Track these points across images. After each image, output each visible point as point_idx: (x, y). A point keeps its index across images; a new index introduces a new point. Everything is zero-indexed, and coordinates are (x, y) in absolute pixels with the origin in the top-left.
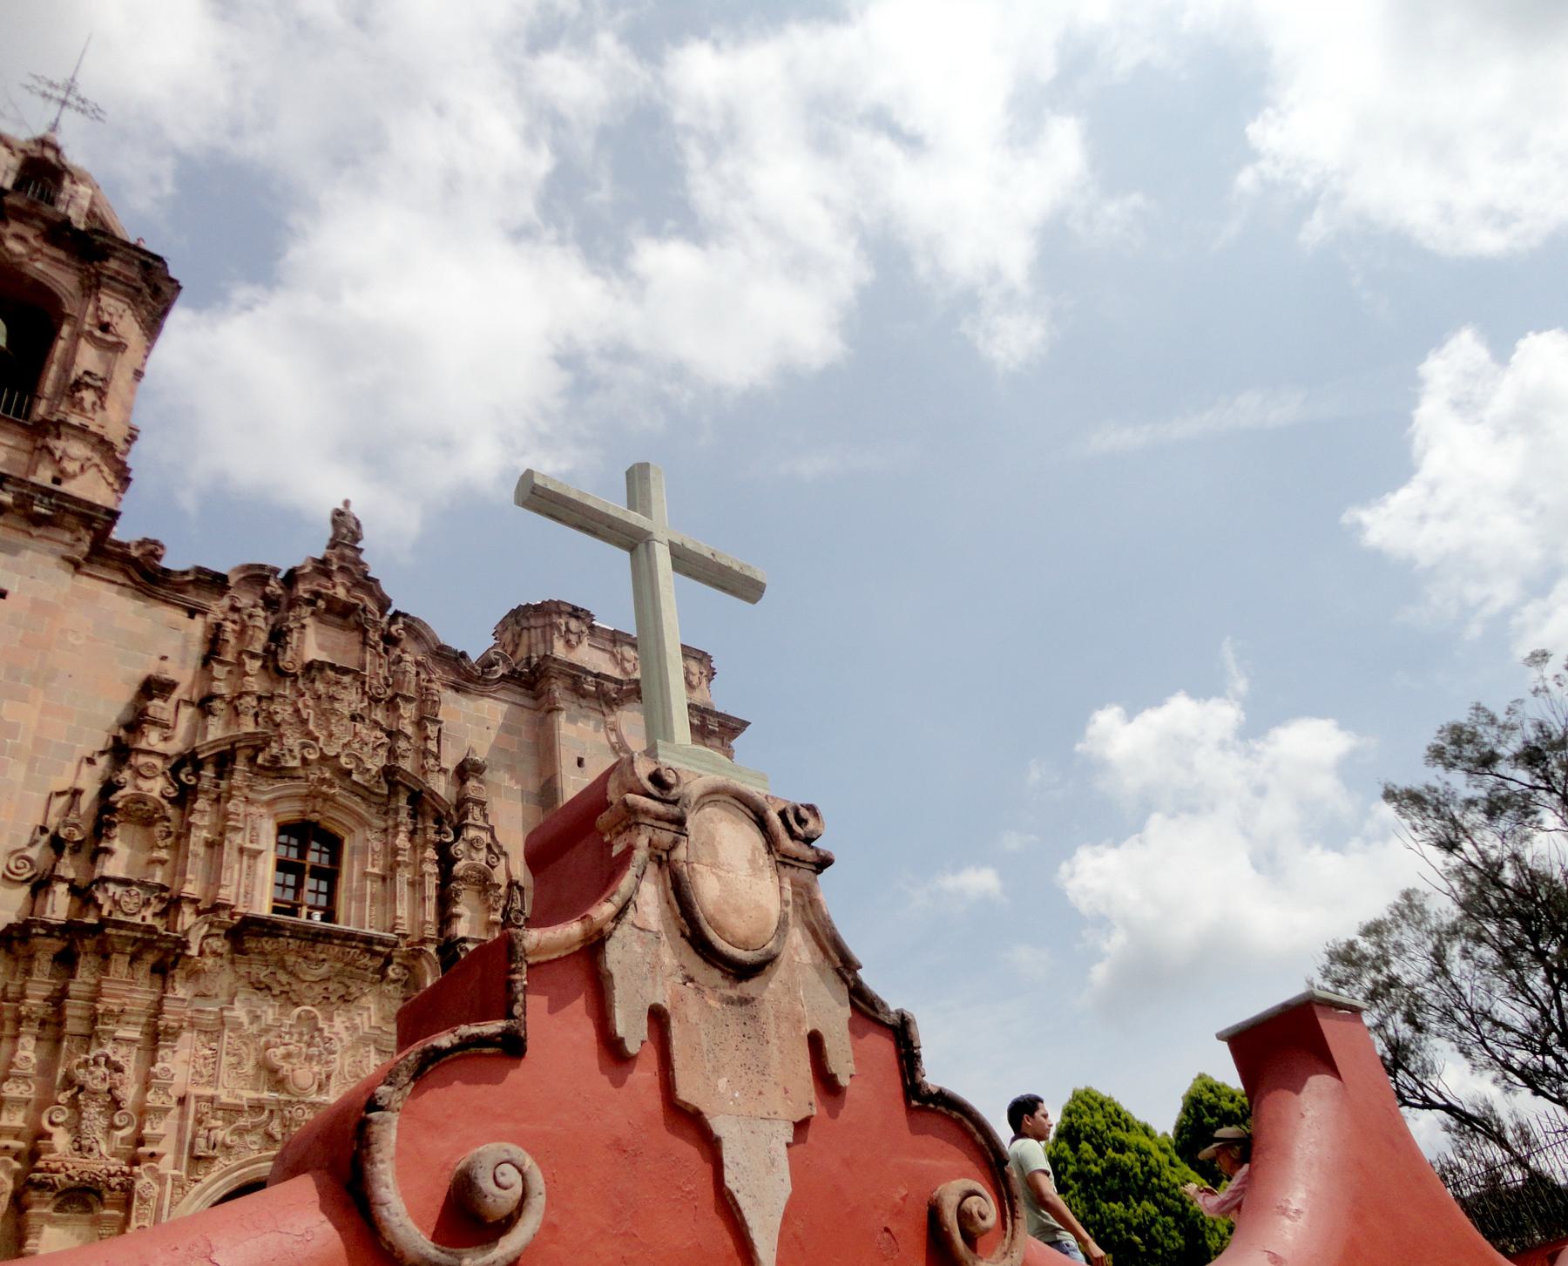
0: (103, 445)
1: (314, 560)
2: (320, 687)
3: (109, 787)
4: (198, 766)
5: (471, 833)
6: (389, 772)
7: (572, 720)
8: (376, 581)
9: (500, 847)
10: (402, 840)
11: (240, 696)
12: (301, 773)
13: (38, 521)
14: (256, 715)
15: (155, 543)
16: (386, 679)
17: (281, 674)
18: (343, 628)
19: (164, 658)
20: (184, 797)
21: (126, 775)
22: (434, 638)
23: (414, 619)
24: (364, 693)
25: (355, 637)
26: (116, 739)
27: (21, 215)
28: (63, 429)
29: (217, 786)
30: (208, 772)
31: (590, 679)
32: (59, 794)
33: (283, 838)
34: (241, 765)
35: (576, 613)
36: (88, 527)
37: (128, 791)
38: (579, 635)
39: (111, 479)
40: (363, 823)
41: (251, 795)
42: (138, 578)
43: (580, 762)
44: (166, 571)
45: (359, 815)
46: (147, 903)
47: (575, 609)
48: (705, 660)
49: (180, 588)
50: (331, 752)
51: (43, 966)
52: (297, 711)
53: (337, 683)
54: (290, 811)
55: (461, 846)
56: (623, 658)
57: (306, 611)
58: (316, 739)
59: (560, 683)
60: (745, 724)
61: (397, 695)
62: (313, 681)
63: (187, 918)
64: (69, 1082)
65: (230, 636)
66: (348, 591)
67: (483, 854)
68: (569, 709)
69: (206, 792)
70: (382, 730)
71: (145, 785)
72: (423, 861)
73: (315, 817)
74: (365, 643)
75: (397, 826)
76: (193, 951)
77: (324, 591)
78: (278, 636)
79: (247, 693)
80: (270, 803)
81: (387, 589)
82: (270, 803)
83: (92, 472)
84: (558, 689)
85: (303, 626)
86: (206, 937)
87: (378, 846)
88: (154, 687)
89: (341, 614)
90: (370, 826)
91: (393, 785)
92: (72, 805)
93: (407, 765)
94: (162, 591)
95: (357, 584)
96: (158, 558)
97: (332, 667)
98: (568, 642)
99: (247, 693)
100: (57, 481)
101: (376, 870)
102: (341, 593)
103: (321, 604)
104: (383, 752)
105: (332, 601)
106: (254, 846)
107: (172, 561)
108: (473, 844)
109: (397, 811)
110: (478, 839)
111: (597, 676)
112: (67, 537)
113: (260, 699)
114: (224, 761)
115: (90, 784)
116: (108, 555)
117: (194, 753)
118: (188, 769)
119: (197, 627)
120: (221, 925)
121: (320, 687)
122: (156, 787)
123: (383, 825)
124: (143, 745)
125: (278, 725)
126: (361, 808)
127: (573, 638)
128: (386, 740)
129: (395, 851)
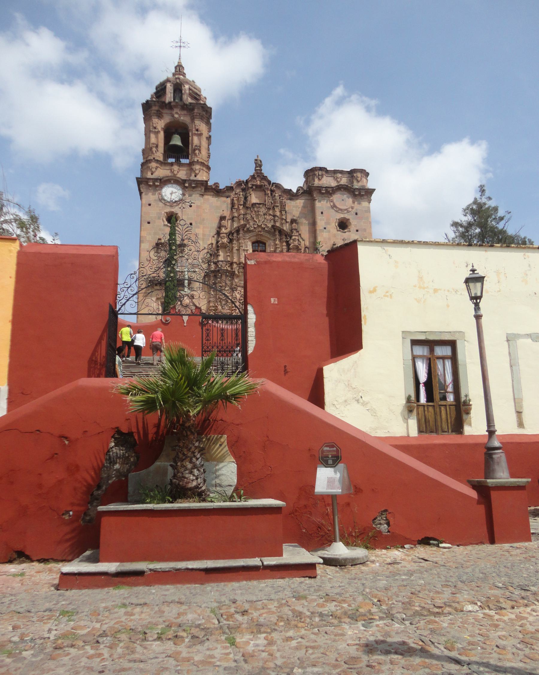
0: (202, 164)
1: (251, 176)
2: (256, 209)
3: (217, 242)
4: (233, 234)
5: (293, 237)
6: (273, 226)
7: (320, 201)
8: (266, 177)
9: (302, 238)
10: (277, 242)
11: (240, 215)
12: (254, 230)
13: (194, 188)
14: (244, 219)
15: (217, 183)
16: (271, 202)
17: (247, 208)
18: (261, 191)
19: (223, 211)
20: (231, 241)
21: (220, 239)
22: (283, 187)
23: (278, 184)
24: (266, 208)
25: (263, 193)
26: (217, 231)
27: (176, 106)
28: (194, 163)
29: (237, 237)
30: (235, 235)
31: (324, 189)
32: (209, 245)
33: (254, 245)
34: (241, 232)
35: (321, 169)
36: (203, 186)
37: (220, 242)
38: (322, 175)
39: (206, 170)
40: (269, 239)
41: (245, 238)
42: (216, 193)
43: (322, 213)
44: (220, 189)
45: (267, 237)
46: (226, 265)
47: (320, 168)
48: (363, 172)
49: (224, 192)
50: (259, 224)
51: (212, 278)
52: (252, 216)
53: (259, 207)
54: (254, 239)
55: (291, 241)
56: (337, 178)
57: (251, 190)
58: (256, 222)
59: (316, 192)
60: (374, 190)
61: (274, 206)
62: (254, 208)
63: (235, 266)
64: (219, 298)
65: (236, 202)
66: (260, 181)
67: (297, 242)
68: (319, 199)
69: (235, 239)
70: (272, 215)
71: (223, 240)
72: (283, 246)
73: (259, 239)
74: (265, 194)
75: (276, 239)
76: (237, 272)
77: (255, 183)
78: (246, 198)
79: (241, 214)
80: (249, 238)
81: (269, 178)
82: (249, 238)
83: (201, 171)
84: (315, 195)
85: (251, 194)
86: (238, 270)
87: (273, 244)
88: (222, 218)
89: (259, 188)
90: (271, 240)
91: (274, 229)
92: (212, 246)
93: (278, 224)
94: (221, 194)
95: (262, 179)
96: (219, 187)
97: (257, 203)
98: (319, 178)
99: (241, 214)
100: (195, 176)
101: (273, 250)
102: (258, 183)
103: (254, 187)
104: (272, 221)
105: (257, 186)
106: (247, 249)
107: (221, 187)
108: (294, 240)
109: (276, 235)
110: (295, 239)
111: (326, 187)
112: (200, 189)
113: (244, 215)
114: (238, 231)
115: (214, 242)
116: (209, 189)
117: (231, 232)
118: (231, 235)
119: (229, 200)
120: (241, 266)
121: (256, 209)
122: (225, 240)
123: (273, 239)
124: (222, 232)
125: (248, 220)
126: (268, 236)
127: (320, 177)
128: (273, 218)
129: (276, 245)
